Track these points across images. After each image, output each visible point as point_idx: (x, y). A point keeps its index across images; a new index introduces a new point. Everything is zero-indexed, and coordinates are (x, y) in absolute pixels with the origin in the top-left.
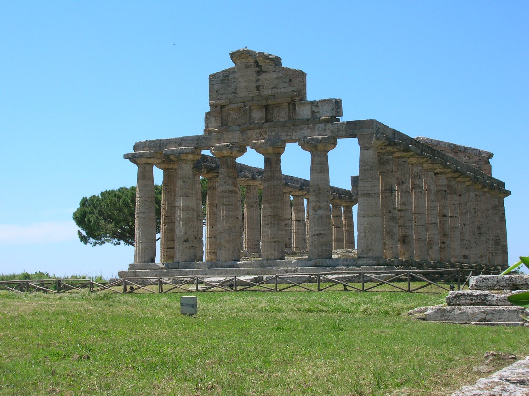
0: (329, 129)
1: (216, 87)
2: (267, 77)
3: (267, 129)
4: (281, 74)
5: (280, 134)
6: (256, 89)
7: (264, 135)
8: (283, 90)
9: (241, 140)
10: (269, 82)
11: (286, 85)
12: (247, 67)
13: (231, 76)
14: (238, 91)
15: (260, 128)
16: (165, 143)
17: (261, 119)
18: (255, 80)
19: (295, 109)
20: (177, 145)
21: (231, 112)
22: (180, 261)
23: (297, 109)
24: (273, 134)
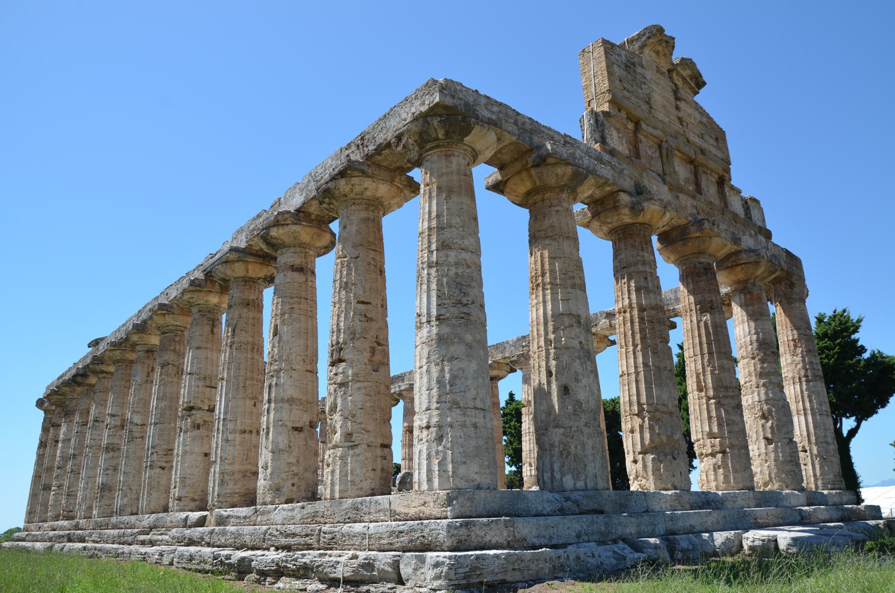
4: (704, 120)
11: (715, 143)
15: (694, 197)
17: (687, 181)
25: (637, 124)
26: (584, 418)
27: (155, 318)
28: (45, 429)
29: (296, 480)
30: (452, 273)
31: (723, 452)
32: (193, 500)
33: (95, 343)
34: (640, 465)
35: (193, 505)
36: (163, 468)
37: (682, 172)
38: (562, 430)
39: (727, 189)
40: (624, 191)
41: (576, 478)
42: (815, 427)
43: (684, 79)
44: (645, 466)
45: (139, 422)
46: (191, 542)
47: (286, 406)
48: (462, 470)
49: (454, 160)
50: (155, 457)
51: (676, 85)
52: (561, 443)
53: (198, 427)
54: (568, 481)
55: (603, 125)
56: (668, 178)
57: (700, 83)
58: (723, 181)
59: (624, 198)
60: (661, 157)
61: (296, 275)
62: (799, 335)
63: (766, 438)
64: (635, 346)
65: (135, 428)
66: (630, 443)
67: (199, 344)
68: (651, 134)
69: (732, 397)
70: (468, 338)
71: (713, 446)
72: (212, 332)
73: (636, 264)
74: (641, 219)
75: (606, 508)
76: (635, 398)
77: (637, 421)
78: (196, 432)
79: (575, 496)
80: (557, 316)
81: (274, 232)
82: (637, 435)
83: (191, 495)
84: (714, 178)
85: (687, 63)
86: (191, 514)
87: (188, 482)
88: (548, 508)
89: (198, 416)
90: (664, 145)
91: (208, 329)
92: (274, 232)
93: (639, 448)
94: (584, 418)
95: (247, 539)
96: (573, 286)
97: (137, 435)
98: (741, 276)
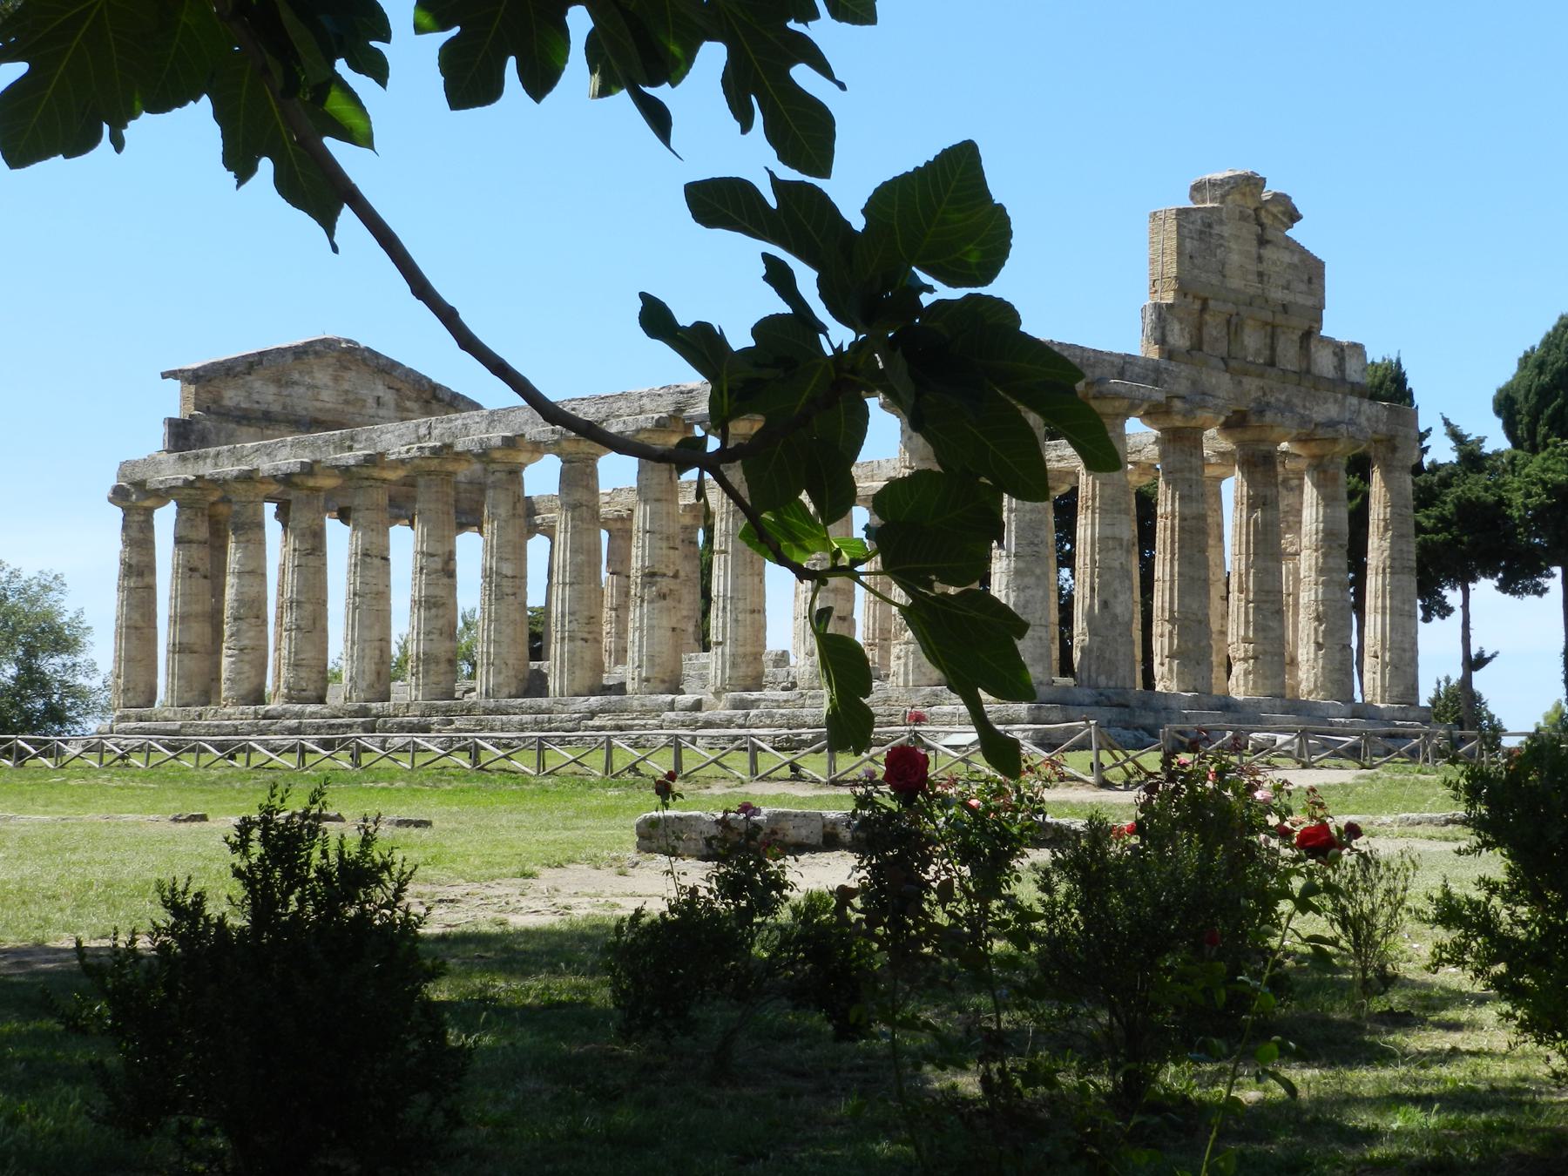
4: (1296, 259)
12: (1243, 217)
13: (1216, 229)
15: (1261, 376)
17: (1258, 353)
25: (1205, 301)
27: (564, 444)
31: (1255, 658)
32: (663, 681)
34: (1166, 667)
35: (662, 687)
36: (586, 640)
37: (1252, 340)
39: (1313, 343)
40: (1178, 397)
41: (1109, 678)
42: (1392, 630)
43: (1275, 216)
44: (1171, 670)
45: (510, 573)
46: (709, 724)
50: (575, 626)
51: (1261, 225)
53: (664, 597)
54: (1102, 680)
56: (1233, 364)
57: (1294, 216)
58: (1310, 334)
59: (1178, 404)
62: (1392, 514)
63: (1317, 643)
64: (1173, 554)
65: (505, 582)
66: (1159, 646)
67: (658, 495)
69: (1273, 602)
70: (1038, 571)
71: (1246, 651)
73: (1182, 471)
74: (1193, 424)
76: (1167, 605)
77: (1168, 627)
78: (664, 603)
79: (1107, 692)
80: (1103, 539)
82: (1166, 640)
84: (1296, 337)
85: (1282, 199)
87: (658, 660)
88: (1087, 700)
89: (664, 584)
90: (1234, 320)
93: (1166, 652)
95: (809, 720)
96: (1119, 512)
97: (509, 591)
98: (1316, 451)
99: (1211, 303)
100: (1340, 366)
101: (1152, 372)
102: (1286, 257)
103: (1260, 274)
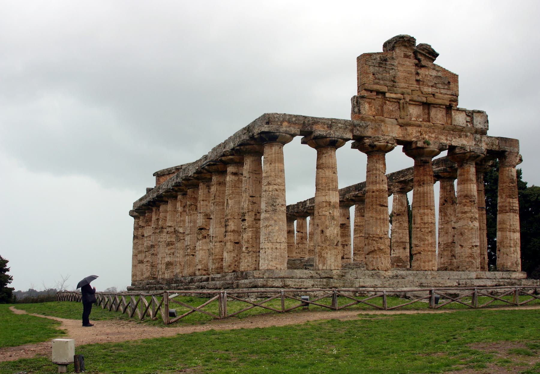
0: (484, 141)
1: (372, 69)
2: (427, 73)
3: (428, 129)
4: (440, 74)
5: (440, 137)
6: (415, 83)
7: (424, 135)
8: (442, 91)
9: (401, 136)
10: (429, 79)
14: (397, 80)
15: (420, 126)
16: (311, 122)
17: (418, 117)
18: (414, 73)
19: (451, 114)
20: (326, 126)
21: (387, 102)
22: (333, 268)
23: (453, 114)
24: (433, 135)
26: (328, 243)
28: (136, 229)
29: (236, 264)
30: (270, 194)
33: (159, 175)
38: (320, 247)
45: (182, 232)
47: (232, 234)
48: (271, 263)
49: (274, 148)
52: (319, 252)
53: (205, 237)
55: (360, 103)
58: (450, 107)
60: (399, 108)
61: (233, 177)
68: (393, 98)
72: (209, 192)
75: (334, 277)
78: (204, 240)
81: (223, 158)
83: (205, 268)
86: (203, 277)
90: (401, 101)
91: (207, 190)
92: (223, 158)
94: (328, 243)
97: (182, 238)
99: (387, 95)
100: (472, 122)
101: (350, 126)
102: (434, 73)
103: (417, 81)
